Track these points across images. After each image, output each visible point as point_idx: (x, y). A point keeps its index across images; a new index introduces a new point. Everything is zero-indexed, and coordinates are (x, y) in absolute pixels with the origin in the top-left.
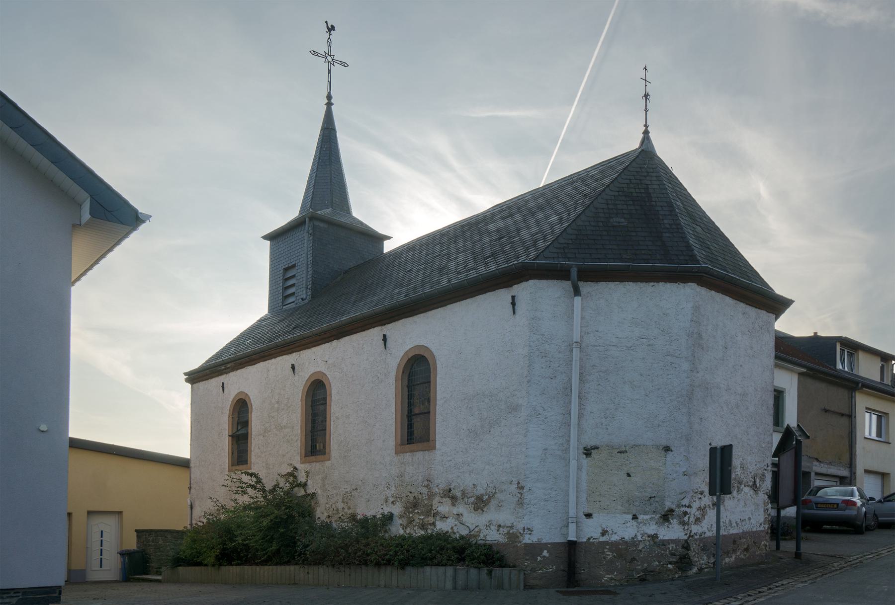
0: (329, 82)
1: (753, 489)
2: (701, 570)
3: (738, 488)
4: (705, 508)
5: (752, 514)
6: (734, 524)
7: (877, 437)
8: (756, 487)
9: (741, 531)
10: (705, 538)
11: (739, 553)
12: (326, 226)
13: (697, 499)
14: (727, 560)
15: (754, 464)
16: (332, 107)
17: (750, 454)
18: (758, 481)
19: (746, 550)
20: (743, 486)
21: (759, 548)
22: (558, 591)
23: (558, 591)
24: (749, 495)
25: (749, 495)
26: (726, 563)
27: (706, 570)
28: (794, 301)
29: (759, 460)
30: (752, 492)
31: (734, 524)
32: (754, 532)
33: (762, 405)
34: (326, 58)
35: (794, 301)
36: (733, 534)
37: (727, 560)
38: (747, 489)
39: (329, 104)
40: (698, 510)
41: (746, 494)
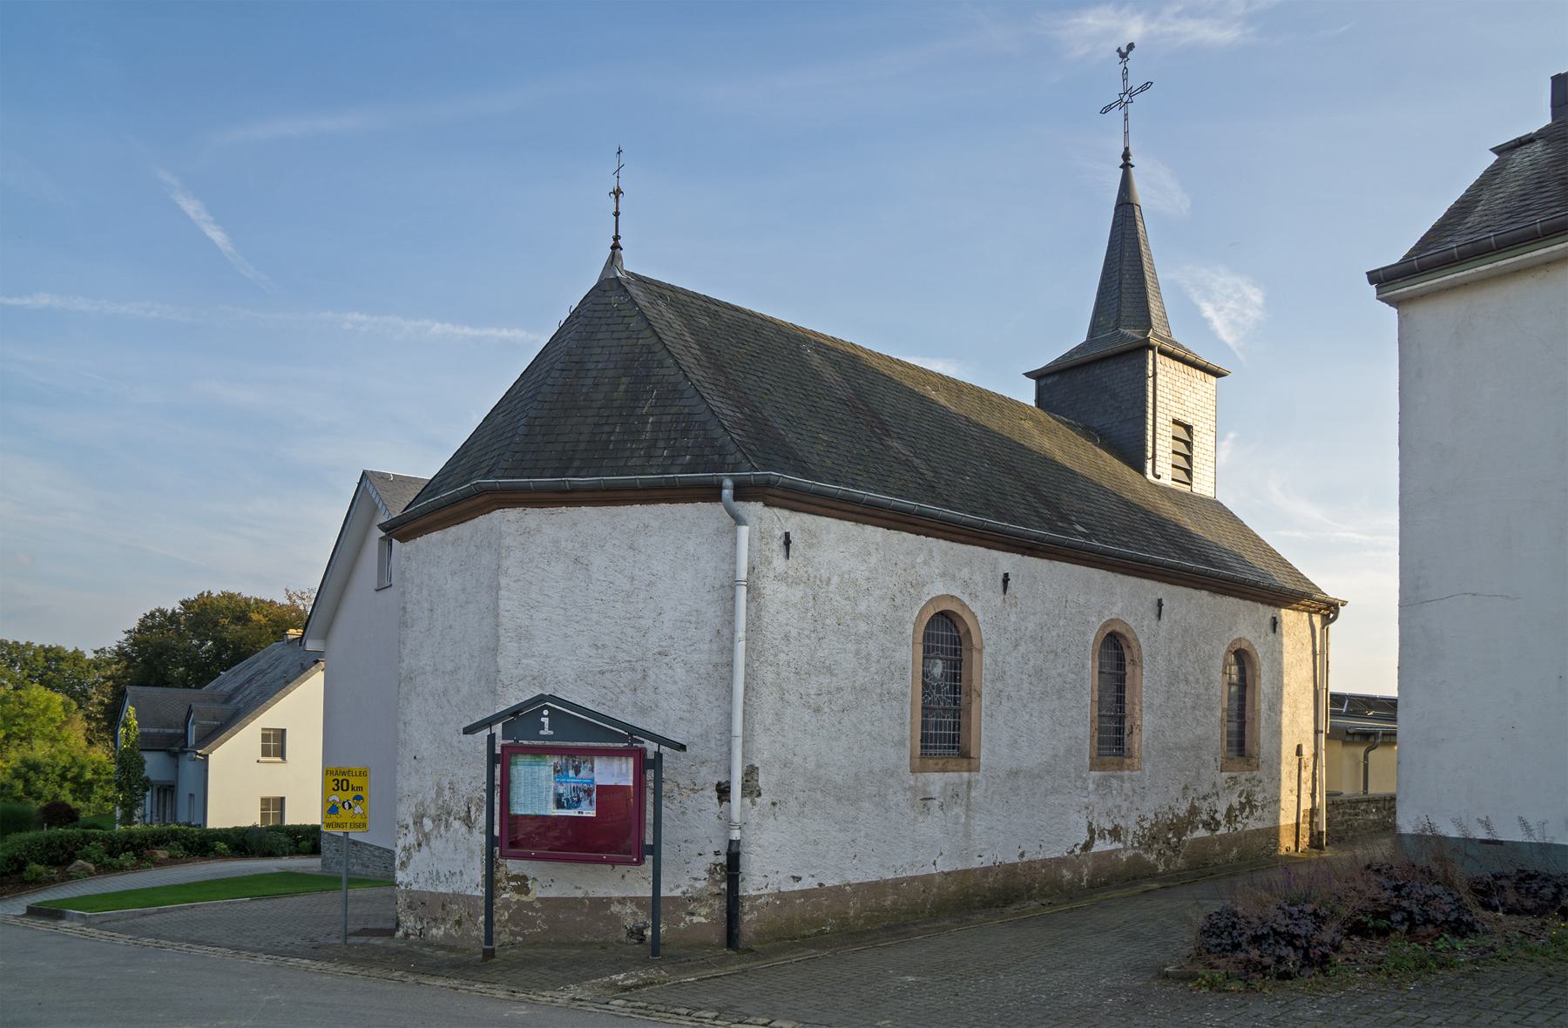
0: (1126, 133)
1: (467, 825)
2: (407, 935)
3: (447, 821)
4: (410, 848)
5: (464, 866)
6: (443, 879)
7: (263, 756)
8: (471, 822)
9: (451, 891)
10: (410, 891)
11: (448, 926)
12: (1056, 378)
13: (401, 836)
14: (434, 931)
15: (468, 782)
16: (1132, 169)
17: (462, 765)
18: (473, 809)
19: (459, 923)
20: (452, 818)
21: (476, 925)
22: (33, 912)
23: (33, 912)
24: (460, 833)
25: (460, 833)
26: (432, 935)
27: (412, 937)
28: (1491, 150)
29: (476, 775)
30: (464, 829)
31: (443, 879)
32: (468, 896)
33: (479, 679)
34: (1125, 94)
35: (1491, 150)
36: (441, 893)
37: (434, 931)
38: (457, 824)
39: (1126, 166)
40: (403, 850)
41: (456, 831)
